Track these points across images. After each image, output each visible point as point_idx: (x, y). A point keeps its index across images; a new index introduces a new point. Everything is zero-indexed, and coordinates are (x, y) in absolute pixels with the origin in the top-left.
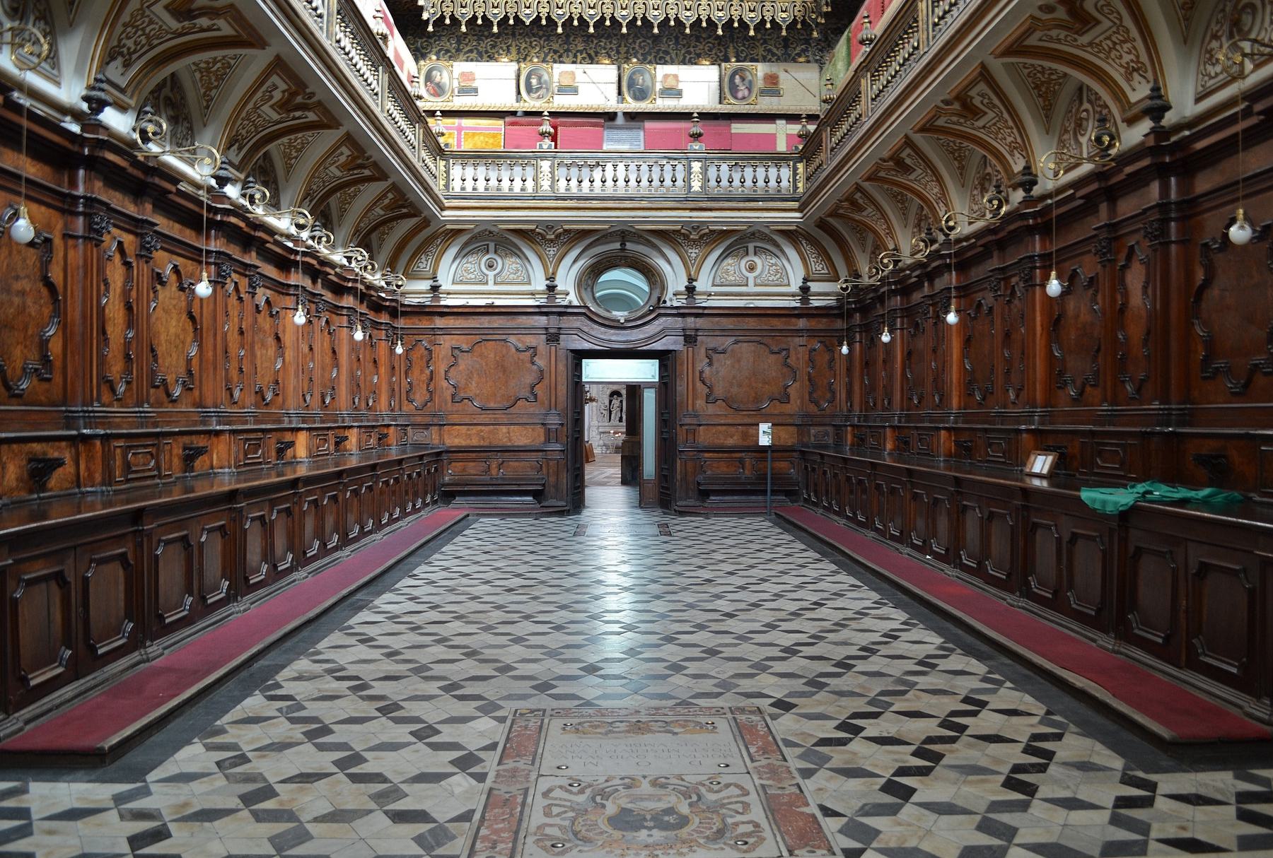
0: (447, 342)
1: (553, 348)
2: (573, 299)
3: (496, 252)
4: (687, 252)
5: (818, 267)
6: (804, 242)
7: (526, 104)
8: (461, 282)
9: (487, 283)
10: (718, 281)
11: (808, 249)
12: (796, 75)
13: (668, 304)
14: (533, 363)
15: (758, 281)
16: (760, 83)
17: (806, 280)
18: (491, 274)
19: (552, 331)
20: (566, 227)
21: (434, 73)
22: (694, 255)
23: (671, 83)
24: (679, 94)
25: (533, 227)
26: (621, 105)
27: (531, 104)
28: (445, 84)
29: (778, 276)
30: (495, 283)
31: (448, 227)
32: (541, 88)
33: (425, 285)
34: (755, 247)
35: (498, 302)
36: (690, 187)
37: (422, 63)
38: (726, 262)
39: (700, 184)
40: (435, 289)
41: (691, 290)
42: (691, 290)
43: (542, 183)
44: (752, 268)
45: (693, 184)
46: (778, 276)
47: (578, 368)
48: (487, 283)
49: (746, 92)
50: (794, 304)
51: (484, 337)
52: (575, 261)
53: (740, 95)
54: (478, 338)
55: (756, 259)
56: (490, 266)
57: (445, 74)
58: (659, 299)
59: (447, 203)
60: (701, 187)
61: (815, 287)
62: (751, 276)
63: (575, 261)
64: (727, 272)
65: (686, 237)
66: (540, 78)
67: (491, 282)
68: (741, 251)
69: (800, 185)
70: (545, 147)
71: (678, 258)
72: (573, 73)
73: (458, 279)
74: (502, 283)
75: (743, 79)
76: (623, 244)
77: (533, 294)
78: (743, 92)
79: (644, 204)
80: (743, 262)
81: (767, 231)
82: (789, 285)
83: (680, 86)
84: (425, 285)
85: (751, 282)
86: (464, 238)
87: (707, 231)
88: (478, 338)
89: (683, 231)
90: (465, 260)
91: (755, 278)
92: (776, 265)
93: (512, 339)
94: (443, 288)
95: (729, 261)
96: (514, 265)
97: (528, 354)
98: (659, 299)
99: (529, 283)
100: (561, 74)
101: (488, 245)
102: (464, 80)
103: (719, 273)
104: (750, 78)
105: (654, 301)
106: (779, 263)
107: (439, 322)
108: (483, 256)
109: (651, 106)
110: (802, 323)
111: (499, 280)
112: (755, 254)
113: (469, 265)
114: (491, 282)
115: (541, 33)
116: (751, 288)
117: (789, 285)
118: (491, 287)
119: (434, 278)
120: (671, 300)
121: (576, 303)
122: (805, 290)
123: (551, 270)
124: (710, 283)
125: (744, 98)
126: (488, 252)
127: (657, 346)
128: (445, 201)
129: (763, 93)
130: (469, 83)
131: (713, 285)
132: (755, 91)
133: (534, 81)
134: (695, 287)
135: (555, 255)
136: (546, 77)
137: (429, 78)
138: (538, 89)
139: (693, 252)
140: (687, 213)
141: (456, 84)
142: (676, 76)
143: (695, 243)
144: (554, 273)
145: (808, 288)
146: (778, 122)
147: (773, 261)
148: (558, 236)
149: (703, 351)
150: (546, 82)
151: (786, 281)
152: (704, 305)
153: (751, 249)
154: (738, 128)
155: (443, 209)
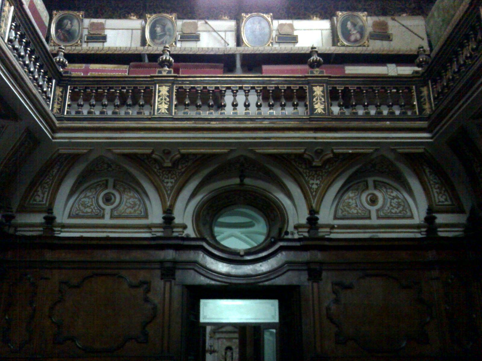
0: (57, 276)
1: (168, 284)
2: (190, 232)
3: (114, 187)
4: (308, 183)
5: (441, 198)
6: (427, 171)
7: (150, 48)
8: (77, 216)
9: (103, 217)
10: (340, 214)
11: (431, 178)
12: (404, 22)
13: (290, 236)
14: (147, 300)
15: (381, 214)
16: (369, 29)
17: (430, 210)
18: (108, 209)
19: (168, 265)
20: (183, 151)
21: (65, 21)
22: (315, 187)
23: (286, 30)
24: (294, 39)
25: (148, 151)
26: (239, 48)
27: (153, 48)
28: (75, 30)
29: (401, 209)
30: (112, 217)
31: (62, 151)
32: (165, 34)
33: (39, 219)
34: (375, 181)
35: (112, 235)
36: (313, 109)
37: (55, 12)
38: (345, 197)
39: (322, 107)
40: (50, 220)
41: (313, 221)
42: (313, 221)
43: (160, 106)
44: (373, 201)
45: (316, 106)
46: (401, 209)
47: (195, 310)
48: (103, 217)
49: (358, 36)
50: (419, 236)
51: (95, 271)
52: (193, 195)
53: (353, 38)
54: (88, 272)
55: (377, 193)
56: (108, 200)
57: (75, 22)
58: (280, 230)
59: (57, 124)
60: (324, 110)
61: (441, 219)
62: (373, 209)
63: (193, 195)
64: (349, 205)
65: (308, 163)
66: (164, 27)
67: (107, 216)
68: (362, 185)
69: (427, 106)
70: (164, 74)
71: (299, 190)
72: (196, 25)
73: (74, 212)
74: (119, 217)
75: (354, 25)
76: (242, 181)
77: (149, 227)
78: (355, 35)
79: (266, 124)
80: (364, 196)
81: (391, 156)
82: (412, 217)
83: (295, 33)
84: (39, 219)
85: (374, 215)
86: (79, 168)
87: (331, 155)
88: (88, 272)
89: (305, 156)
90: (82, 196)
91: (378, 211)
92: (397, 198)
93: (123, 273)
94: (59, 220)
95: (350, 194)
96: (131, 201)
97: (141, 290)
98: (280, 230)
99: (146, 217)
100: (183, 25)
101: (107, 181)
102: (93, 29)
103: (341, 206)
104: (361, 24)
105: (275, 233)
106: (400, 195)
107: (49, 256)
108: (102, 191)
109: (269, 48)
110: (431, 255)
111: (115, 213)
112: (375, 187)
113: (87, 200)
114: (107, 216)
115: (169, 5)
116: (374, 221)
117: (412, 217)
118: (107, 220)
119: (50, 210)
120: (293, 234)
121: (193, 235)
122: (430, 219)
123: (168, 204)
124: (332, 216)
125: (356, 41)
126: (106, 187)
127: (280, 281)
128: (56, 122)
129: (374, 36)
130: (99, 32)
131: (335, 218)
132: (367, 34)
133: (158, 29)
134: (317, 219)
135: (172, 187)
136: (169, 25)
137: (59, 26)
138: (162, 36)
139: (314, 184)
140: (311, 134)
141: (86, 32)
142: (291, 26)
143: (316, 171)
144: (172, 207)
145: (435, 218)
146: (389, 65)
147: (394, 194)
148: (175, 164)
149: (329, 288)
150: (169, 29)
151: (409, 214)
152: (327, 237)
153: (370, 181)
154: (351, 70)
155: (54, 130)
